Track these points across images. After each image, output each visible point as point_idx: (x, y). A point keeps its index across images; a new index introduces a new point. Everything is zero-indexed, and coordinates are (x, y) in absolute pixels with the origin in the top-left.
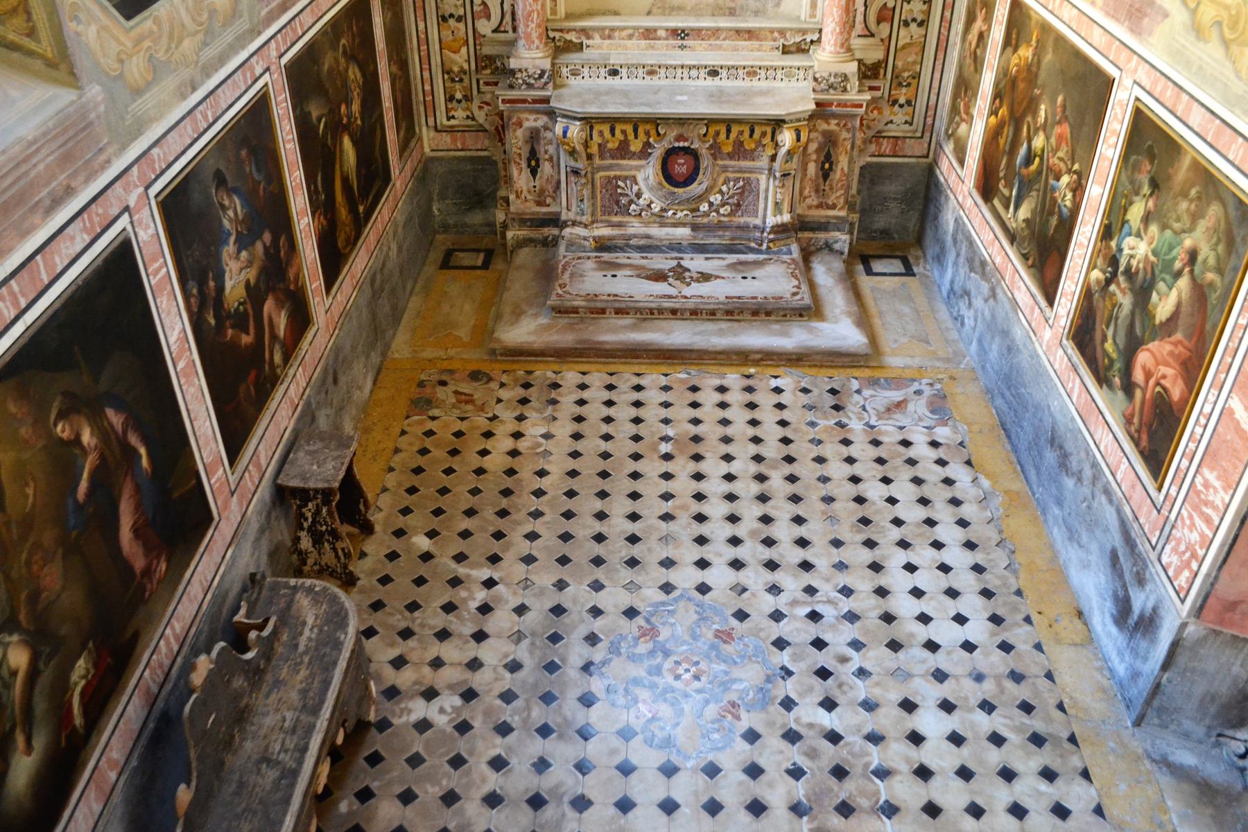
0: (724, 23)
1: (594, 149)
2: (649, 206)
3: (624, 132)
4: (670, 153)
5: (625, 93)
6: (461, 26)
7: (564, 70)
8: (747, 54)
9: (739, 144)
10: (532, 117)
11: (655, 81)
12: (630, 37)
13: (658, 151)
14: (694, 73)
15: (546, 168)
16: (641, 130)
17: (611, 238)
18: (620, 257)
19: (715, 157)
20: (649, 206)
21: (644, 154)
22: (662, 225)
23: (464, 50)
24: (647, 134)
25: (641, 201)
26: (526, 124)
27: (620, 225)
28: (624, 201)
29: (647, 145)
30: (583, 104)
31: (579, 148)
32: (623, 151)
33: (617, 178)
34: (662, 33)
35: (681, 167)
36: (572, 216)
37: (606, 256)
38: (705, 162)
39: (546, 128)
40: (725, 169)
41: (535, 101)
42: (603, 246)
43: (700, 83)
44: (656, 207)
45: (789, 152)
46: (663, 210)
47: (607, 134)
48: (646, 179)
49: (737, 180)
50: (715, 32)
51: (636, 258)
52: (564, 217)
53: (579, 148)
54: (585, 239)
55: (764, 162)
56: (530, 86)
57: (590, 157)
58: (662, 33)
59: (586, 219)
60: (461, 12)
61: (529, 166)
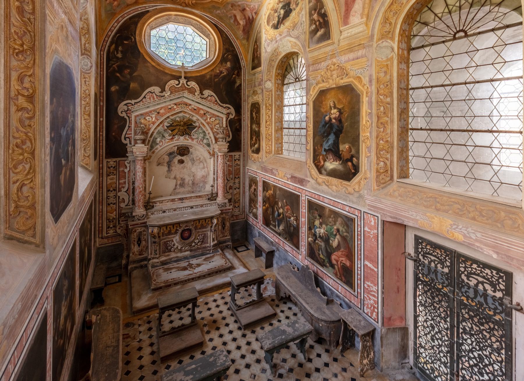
0: (193, 195)
1: (161, 235)
2: (177, 248)
3: (170, 228)
4: (183, 231)
5: (169, 217)
6: (115, 206)
7: (149, 214)
8: (200, 202)
9: (202, 225)
10: (139, 229)
11: (176, 212)
12: (168, 202)
13: (180, 231)
14: (187, 208)
15: (144, 243)
16: (175, 226)
17: (166, 260)
18: (170, 266)
19: (196, 230)
20: (177, 248)
21: (176, 233)
22: (181, 252)
23: (115, 212)
24: (177, 227)
25: (175, 247)
26: (137, 231)
27: (168, 255)
28: (169, 248)
29: (177, 230)
30: (158, 222)
31: (157, 235)
32: (170, 233)
33: (167, 241)
34: (177, 200)
35: (186, 234)
36: (152, 256)
37: (166, 267)
38: (193, 232)
39: (144, 231)
40: (199, 232)
41: (141, 224)
42: (163, 263)
43: (189, 211)
44: (179, 248)
45: (216, 225)
46: (181, 248)
47: (165, 229)
48: (176, 240)
49: (202, 235)
50: (191, 197)
51: (175, 265)
52: (149, 257)
53: (157, 235)
54: (158, 262)
55: (209, 228)
56: (139, 220)
57: (159, 237)
58: (177, 200)
59: (157, 256)
60: (115, 202)
61: (138, 243)
